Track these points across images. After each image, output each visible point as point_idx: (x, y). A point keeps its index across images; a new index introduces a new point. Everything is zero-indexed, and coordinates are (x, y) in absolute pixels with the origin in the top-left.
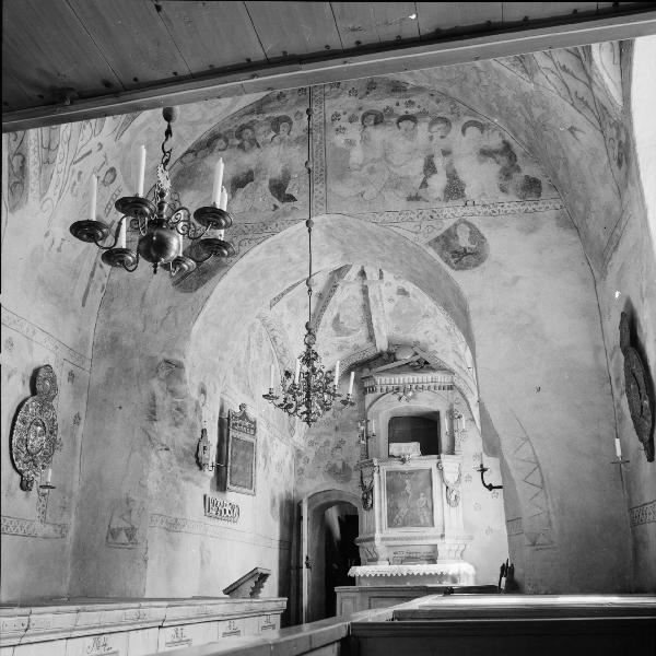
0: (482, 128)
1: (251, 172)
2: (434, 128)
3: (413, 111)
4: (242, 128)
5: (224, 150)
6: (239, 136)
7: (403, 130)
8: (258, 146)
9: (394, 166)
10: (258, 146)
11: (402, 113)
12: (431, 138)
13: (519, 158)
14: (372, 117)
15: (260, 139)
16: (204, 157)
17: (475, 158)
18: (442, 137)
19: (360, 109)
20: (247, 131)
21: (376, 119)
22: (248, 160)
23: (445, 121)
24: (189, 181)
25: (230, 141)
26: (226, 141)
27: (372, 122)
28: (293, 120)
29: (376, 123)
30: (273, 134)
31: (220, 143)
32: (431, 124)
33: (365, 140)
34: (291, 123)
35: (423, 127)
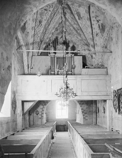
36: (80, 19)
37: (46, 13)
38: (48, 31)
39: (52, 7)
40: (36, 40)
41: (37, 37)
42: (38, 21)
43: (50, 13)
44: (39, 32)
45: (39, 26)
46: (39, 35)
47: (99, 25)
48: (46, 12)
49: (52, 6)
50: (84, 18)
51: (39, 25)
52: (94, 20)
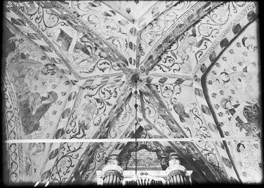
36: (185, 118)
37: (100, 109)
38: (101, 154)
39: (115, 97)
40: (61, 174)
41: (68, 164)
42: (77, 121)
43: (109, 108)
44: (76, 153)
45: (78, 136)
46: (75, 162)
47: (238, 118)
48: (99, 106)
49: (116, 92)
50: (194, 113)
51: (79, 133)
52: (221, 114)
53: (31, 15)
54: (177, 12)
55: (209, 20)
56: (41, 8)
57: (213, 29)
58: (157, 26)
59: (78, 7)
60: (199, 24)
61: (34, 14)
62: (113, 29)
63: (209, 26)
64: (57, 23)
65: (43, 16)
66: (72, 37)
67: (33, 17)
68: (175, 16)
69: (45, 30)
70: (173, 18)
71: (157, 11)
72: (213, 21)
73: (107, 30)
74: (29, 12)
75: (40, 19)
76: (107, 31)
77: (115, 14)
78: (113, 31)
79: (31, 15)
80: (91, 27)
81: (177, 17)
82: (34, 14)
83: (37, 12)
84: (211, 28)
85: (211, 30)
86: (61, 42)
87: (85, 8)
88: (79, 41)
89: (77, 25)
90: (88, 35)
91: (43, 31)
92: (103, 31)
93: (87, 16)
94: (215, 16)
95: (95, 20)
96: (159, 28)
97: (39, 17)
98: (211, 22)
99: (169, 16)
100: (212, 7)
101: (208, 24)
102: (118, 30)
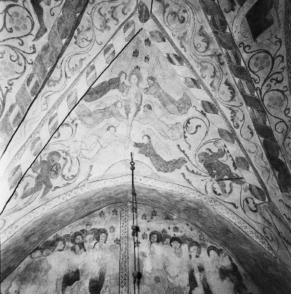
0: (219, 252)
1: (78, 271)
2: (192, 249)
3: (178, 234)
4: (76, 234)
5: (61, 250)
6: (73, 241)
7: (172, 249)
8: (85, 251)
9: (170, 277)
10: (85, 251)
11: (172, 235)
12: (190, 256)
13: (243, 278)
14: (155, 236)
15: (86, 245)
16: (48, 255)
17: (218, 275)
18: (197, 257)
19: (149, 229)
20: (79, 237)
21: (158, 238)
22: (78, 260)
23: (197, 244)
24: (33, 275)
25: (67, 243)
26: (64, 243)
27: (155, 240)
28: (109, 232)
29: (158, 241)
30: (96, 241)
31: (60, 245)
32: (190, 246)
33: (152, 253)
34: (107, 235)
35: (185, 247)
53: (282, 92)
54: (78, 50)
55: (19, 47)
56: (264, 91)
57: (4, 29)
58: (105, 14)
59: (215, 72)
60: (34, 32)
61: (278, 90)
62: (175, 14)
63: (16, 34)
64: (254, 53)
65: (268, 78)
66: (245, 19)
67: (281, 88)
68: (79, 41)
69: (279, 56)
70: (81, 37)
71: (107, 56)
72: (13, 48)
73: (185, 15)
74: (283, 99)
75: (275, 76)
76: (185, 11)
77: (168, 55)
78: (175, 10)
79: (282, 92)
80: (209, 30)
81: (75, 40)
82: (278, 90)
83: (272, 88)
84: (11, 31)
85: (9, 26)
86: (268, 17)
87: (206, 68)
88: (238, 6)
89: (229, 51)
90: (218, 24)
91: (283, 57)
92: (192, 15)
93: (209, 53)
94: (13, 59)
95: (199, 40)
96: (102, 11)
97: (274, 82)
98: (15, 43)
99: (89, 39)
100: (27, 87)
101: (18, 38)
102: (167, 10)
